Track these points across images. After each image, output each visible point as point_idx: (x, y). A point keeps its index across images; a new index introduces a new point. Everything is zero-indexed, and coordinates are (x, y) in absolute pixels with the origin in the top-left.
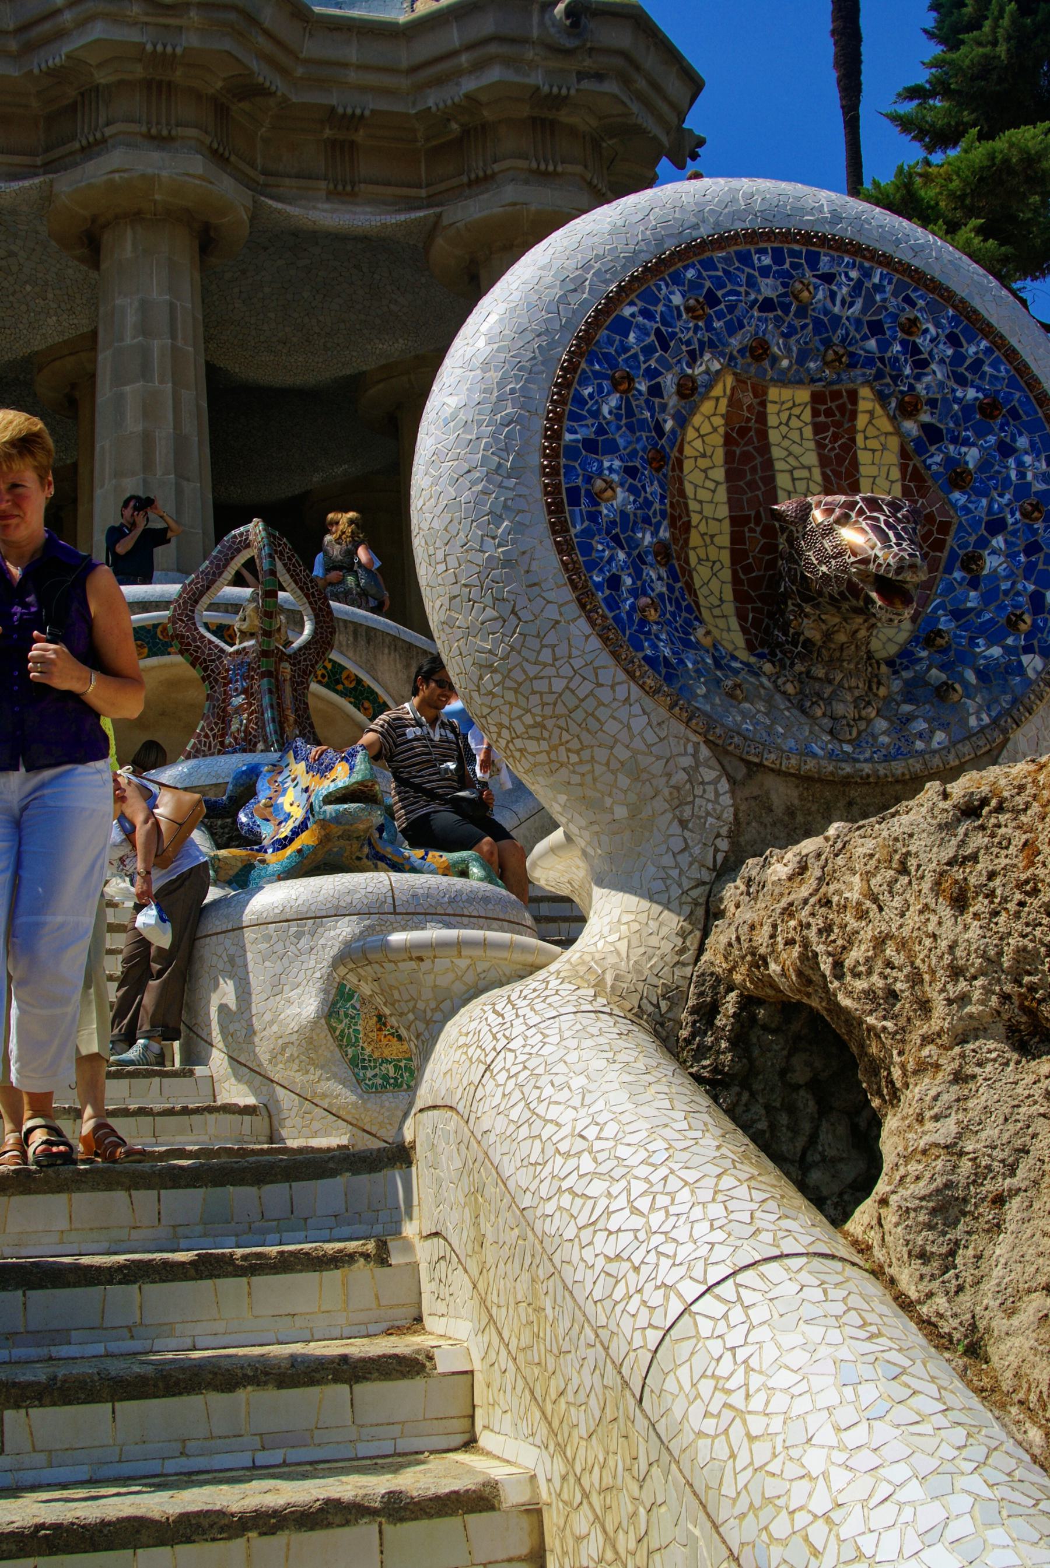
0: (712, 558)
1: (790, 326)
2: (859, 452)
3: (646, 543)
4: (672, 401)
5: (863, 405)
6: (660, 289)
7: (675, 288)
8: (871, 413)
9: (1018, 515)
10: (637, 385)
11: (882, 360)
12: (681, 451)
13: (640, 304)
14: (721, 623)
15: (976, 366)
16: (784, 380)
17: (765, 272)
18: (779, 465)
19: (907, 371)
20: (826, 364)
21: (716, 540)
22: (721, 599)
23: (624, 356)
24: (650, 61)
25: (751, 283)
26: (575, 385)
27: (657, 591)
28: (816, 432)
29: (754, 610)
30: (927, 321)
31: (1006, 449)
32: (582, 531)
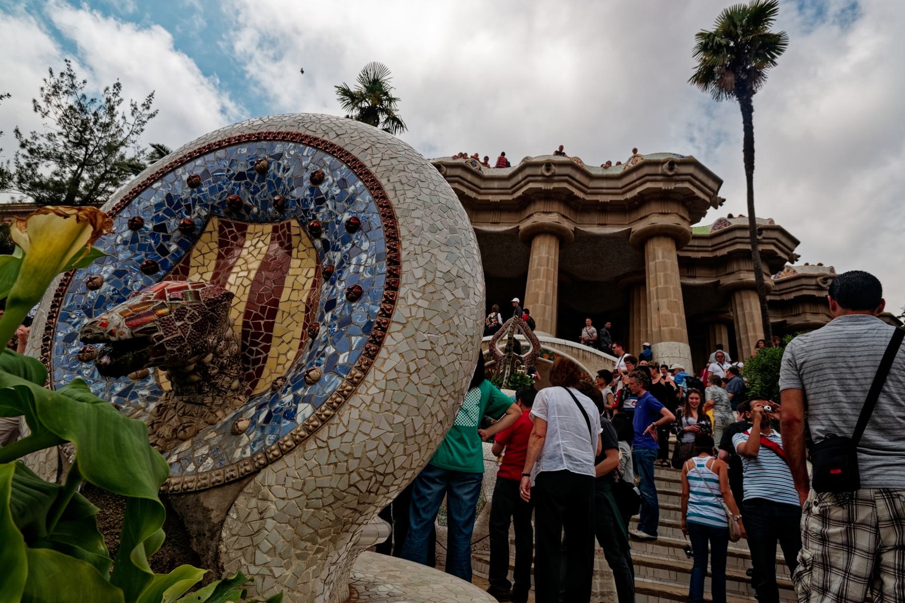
1: (255, 187)
5: (294, 231)
8: (299, 235)
9: (344, 298)
10: (146, 225)
12: (187, 262)
16: (257, 220)
18: (235, 270)
19: (312, 207)
24: (701, 176)
32: (69, 307)
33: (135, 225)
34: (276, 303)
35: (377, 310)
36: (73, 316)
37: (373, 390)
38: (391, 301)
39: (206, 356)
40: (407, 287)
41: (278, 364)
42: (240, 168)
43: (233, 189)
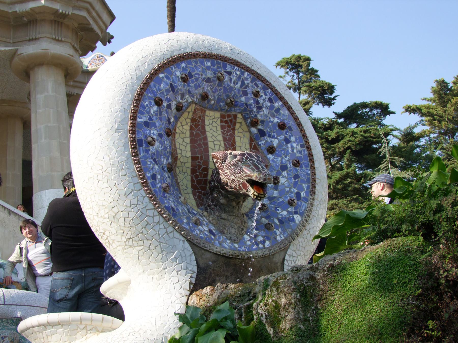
0: (184, 171)
4: (175, 111)
6: (172, 69)
7: (178, 70)
8: (240, 123)
9: (291, 165)
11: (246, 104)
12: (175, 130)
13: (166, 74)
14: (187, 195)
15: (278, 110)
16: (212, 109)
17: (208, 68)
18: (209, 139)
20: (227, 104)
21: (186, 164)
22: (187, 187)
23: (159, 92)
26: (142, 101)
29: (199, 192)
31: (287, 141)
32: (143, 156)
33: (158, 103)
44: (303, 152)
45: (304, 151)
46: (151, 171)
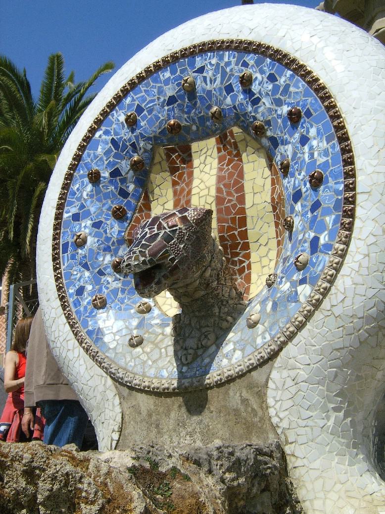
2: (245, 166)
3: (106, 262)
6: (113, 116)
8: (244, 140)
9: (308, 185)
10: (102, 175)
11: (234, 107)
17: (167, 82)
18: (194, 191)
23: (95, 161)
25: (161, 91)
27: (111, 289)
28: (219, 163)
30: (256, 72)
33: (95, 178)
34: (243, 211)
35: (341, 187)
36: (75, 273)
37: (359, 257)
38: (350, 175)
39: (206, 269)
40: (362, 158)
41: (263, 267)
42: (170, 93)
43: (168, 115)
44: (330, 150)
45: (333, 147)
46: (76, 285)
